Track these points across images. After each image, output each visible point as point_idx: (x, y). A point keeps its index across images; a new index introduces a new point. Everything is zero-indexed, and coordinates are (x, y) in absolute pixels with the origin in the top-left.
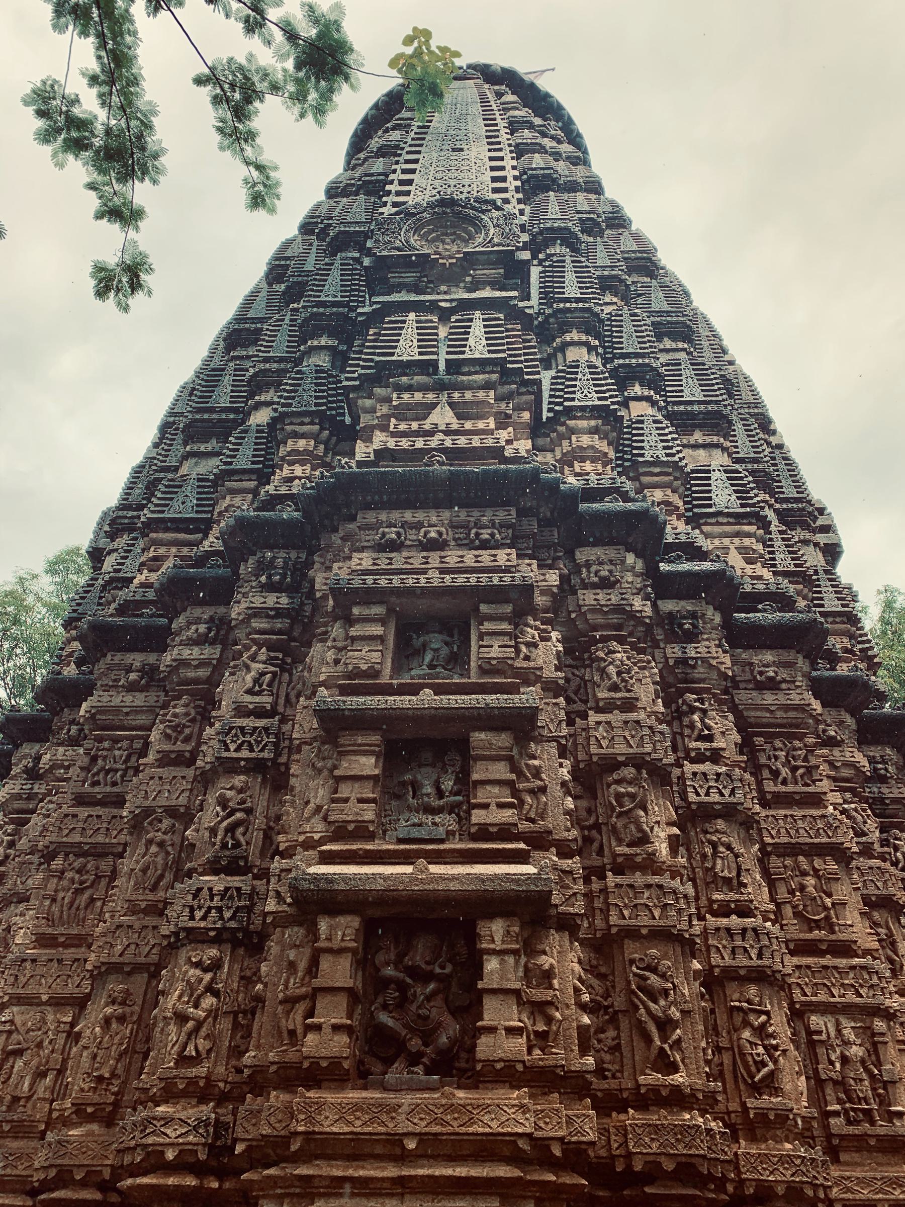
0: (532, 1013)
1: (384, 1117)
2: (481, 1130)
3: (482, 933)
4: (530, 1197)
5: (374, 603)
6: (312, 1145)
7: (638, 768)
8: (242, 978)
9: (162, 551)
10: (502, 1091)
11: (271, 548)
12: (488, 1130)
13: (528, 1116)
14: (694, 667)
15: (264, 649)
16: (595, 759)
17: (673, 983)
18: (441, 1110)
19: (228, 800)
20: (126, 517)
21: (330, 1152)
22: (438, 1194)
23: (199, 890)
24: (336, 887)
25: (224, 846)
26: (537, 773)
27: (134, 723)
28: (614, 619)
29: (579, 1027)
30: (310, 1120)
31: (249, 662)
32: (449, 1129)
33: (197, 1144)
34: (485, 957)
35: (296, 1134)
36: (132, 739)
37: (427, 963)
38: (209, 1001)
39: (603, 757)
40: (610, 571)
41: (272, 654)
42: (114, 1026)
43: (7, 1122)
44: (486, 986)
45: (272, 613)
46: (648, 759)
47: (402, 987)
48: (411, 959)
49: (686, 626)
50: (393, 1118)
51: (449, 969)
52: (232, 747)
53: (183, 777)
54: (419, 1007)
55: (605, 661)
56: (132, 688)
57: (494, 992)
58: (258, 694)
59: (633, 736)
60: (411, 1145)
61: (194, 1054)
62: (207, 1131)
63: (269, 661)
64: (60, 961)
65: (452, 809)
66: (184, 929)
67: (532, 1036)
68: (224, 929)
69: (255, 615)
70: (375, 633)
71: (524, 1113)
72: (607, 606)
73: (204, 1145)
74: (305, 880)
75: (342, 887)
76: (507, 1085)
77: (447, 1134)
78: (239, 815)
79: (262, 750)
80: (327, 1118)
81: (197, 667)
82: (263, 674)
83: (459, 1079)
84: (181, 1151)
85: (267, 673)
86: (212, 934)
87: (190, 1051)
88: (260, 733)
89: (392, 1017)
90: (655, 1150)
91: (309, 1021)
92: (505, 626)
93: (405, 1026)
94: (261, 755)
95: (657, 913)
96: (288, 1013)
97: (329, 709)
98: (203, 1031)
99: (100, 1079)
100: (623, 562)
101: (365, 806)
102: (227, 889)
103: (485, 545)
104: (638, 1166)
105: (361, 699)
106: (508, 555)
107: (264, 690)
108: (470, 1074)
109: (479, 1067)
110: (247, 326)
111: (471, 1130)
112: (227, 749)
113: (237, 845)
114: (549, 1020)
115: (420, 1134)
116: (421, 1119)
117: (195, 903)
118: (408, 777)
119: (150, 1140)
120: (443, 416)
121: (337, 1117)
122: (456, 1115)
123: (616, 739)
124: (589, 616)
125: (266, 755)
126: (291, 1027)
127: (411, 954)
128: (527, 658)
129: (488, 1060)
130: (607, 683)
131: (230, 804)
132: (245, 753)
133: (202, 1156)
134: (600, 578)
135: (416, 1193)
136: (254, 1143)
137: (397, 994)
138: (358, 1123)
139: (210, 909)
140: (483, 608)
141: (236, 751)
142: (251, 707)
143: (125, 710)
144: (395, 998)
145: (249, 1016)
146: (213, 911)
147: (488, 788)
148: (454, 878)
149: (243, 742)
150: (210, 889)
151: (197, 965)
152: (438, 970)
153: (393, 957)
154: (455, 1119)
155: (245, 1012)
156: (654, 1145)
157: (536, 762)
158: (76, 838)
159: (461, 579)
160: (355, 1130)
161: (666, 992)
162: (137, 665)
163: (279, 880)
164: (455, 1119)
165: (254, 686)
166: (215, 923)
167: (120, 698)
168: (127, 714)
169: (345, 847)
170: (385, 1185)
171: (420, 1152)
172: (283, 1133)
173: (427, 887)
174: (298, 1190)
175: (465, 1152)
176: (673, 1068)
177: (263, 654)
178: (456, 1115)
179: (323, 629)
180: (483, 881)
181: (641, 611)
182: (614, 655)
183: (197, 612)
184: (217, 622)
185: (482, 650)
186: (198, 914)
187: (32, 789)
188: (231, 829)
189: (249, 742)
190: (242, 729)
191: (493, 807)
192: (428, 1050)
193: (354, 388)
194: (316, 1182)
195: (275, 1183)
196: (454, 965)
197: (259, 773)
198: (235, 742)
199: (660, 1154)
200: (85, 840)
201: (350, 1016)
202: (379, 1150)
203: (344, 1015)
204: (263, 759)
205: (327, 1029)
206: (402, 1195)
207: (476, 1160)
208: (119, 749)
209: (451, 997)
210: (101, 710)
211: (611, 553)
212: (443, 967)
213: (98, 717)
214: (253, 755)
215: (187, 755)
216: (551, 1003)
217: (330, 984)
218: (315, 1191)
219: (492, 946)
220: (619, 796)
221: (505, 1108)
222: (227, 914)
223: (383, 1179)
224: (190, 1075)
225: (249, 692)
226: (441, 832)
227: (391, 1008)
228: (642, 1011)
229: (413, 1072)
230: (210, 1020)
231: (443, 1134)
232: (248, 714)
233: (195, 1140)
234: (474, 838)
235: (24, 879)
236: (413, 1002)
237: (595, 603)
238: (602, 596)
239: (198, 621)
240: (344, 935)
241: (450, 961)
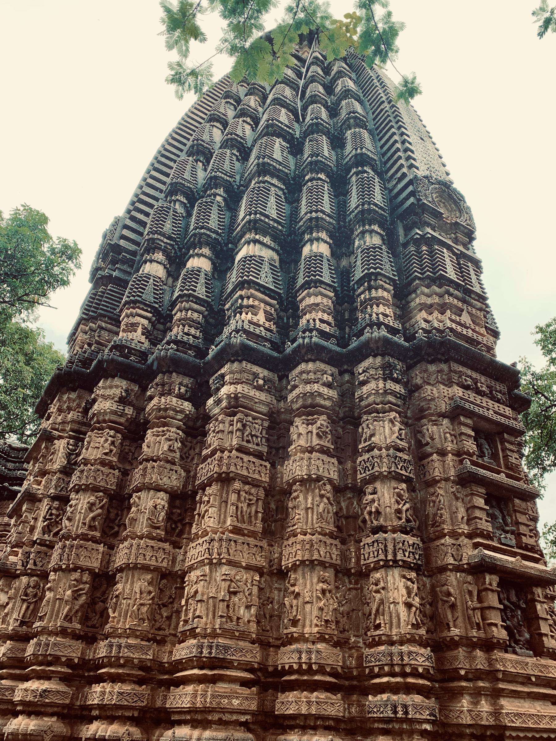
9: (256, 303)
11: (392, 357)
20: (162, 241)
27: (259, 409)
30: (504, 666)
32: (543, 675)
35: (501, 670)
36: (263, 420)
42: (328, 594)
43: (238, 631)
47: (512, 611)
56: (259, 388)
64: (248, 544)
65: (513, 533)
69: (390, 394)
81: (325, 399)
99: (327, 621)
103: (498, 401)
110: (274, 164)
119: (413, 662)
120: (465, 318)
132: (403, 472)
143: (257, 400)
148: (532, 568)
158: (245, 473)
162: (261, 375)
167: (253, 393)
168: (256, 403)
183: (323, 366)
187: (124, 410)
190: (401, 458)
193: (419, 279)
200: (249, 475)
208: (256, 423)
210: (245, 396)
213: (241, 399)
214: (407, 474)
233: (429, 664)
235: (162, 477)
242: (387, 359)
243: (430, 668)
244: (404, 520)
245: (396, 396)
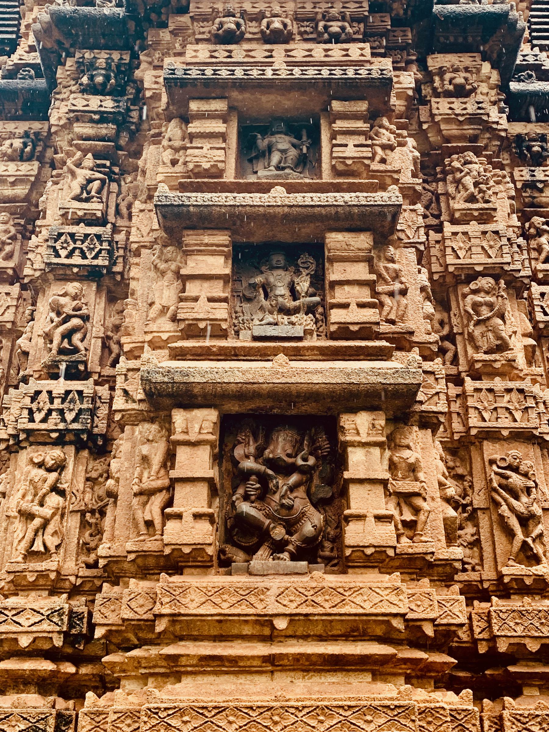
0: (399, 504)
1: (252, 599)
2: (353, 611)
3: (346, 427)
4: (400, 674)
5: (214, 98)
6: (178, 627)
7: (496, 278)
8: (88, 479)
10: (373, 576)
11: (91, 48)
12: (361, 611)
13: (401, 597)
14: (541, 191)
15: (90, 155)
16: (451, 269)
17: (534, 481)
18: (312, 592)
19: (62, 306)
21: (196, 633)
22: (307, 671)
23: (38, 393)
24: (192, 380)
25: (61, 351)
26: (396, 276)
28: (469, 130)
29: (445, 519)
30: (174, 601)
31: (74, 168)
32: (320, 610)
33: (53, 632)
34: (350, 449)
35: (161, 616)
37: (289, 456)
38: (54, 500)
39: (460, 268)
40: (466, 79)
41: (99, 162)
44: (353, 477)
45: (97, 117)
46: (506, 268)
47: (263, 479)
48: (272, 452)
49: (536, 149)
50: (261, 600)
51: (311, 461)
52: (63, 253)
53: (8, 294)
54: (283, 497)
55: (461, 171)
57: (361, 481)
58: (87, 200)
59: (491, 247)
60: (281, 624)
61: (42, 549)
62: (62, 620)
63: (96, 168)
65: (310, 310)
66: (24, 431)
67: (400, 526)
68: (67, 430)
69: (77, 119)
70: (217, 130)
71: (398, 595)
72: (463, 115)
73: (59, 632)
74: (158, 373)
75: (198, 379)
76: (377, 570)
77: (319, 615)
78: (76, 321)
79: (96, 257)
80: (192, 601)
81: (13, 184)
82: (90, 181)
83: (326, 566)
84: (35, 639)
85: (96, 179)
86: (54, 435)
87: (38, 546)
88: (92, 240)
89: (255, 507)
90: (519, 633)
91: (168, 510)
92: (360, 125)
93: (267, 516)
94: (95, 262)
95: (518, 415)
96: (145, 504)
97: (172, 205)
98: (50, 529)
100: (479, 71)
101: (216, 305)
102: (68, 392)
103: (336, 38)
104: (502, 647)
105: (208, 195)
106: (362, 49)
107: (93, 197)
108: (336, 561)
109: (348, 552)
111: (343, 611)
112: (58, 256)
113: (76, 350)
114: (417, 511)
115: (291, 615)
116: (291, 601)
117: (34, 406)
118: (259, 279)
121: (203, 600)
122: (327, 597)
123: (473, 249)
124: (443, 127)
125: (99, 262)
126: (148, 517)
127: (272, 447)
128: (383, 161)
129: (358, 546)
130: (464, 194)
131: (65, 310)
132: (77, 260)
133: (58, 642)
134: (456, 86)
135: (286, 670)
136: (114, 628)
137: (258, 485)
138: (225, 605)
139: (50, 411)
140: (336, 105)
141: (67, 257)
142: (80, 213)
144: (257, 489)
145: (97, 515)
146: (54, 413)
147: (346, 288)
149: (74, 249)
150: (50, 393)
151: (40, 465)
152: (300, 462)
153: (252, 449)
154: (327, 601)
155: (93, 512)
156: (519, 629)
157: (396, 266)
159: (311, 72)
160: (223, 612)
161: (528, 491)
163: (126, 380)
164: (327, 601)
165: (82, 193)
166: (56, 424)
169: (197, 345)
170: (255, 663)
171: (290, 633)
172: (145, 617)
173: (289, 380)
174: (162, 670)
175: (335, 632)
176: (536, 560)
177: (89, 160)
178: (327, 597)
179: (157, 131)
180: (348, 375)
181: (497, 123)
182: (470, 166)
184: (32, 136)
185: (335, 149)
186: (38, 417)
188: (68, 335)
189: (81, 249)
190: (72, 235)
191: (353, 306)
192: (294, 538)
194: (183, 661)
195: (139, 662)
196: (317, 458)
197: (93, 281)
198: (66, 248)
199: (524, 637)
201: (210, 506)
202: (247, 630)
203: (206, 506)
204: (97, 266)
205: (188, 517)
206: (272, 672)
207: (346, 640)
209: (313, 489)
211: (466, 60)
212: (305, 459)
214: (86, 262)
215: (10, 272)
216: (418, 495)
217: (190, 475)
218: (183, 669)
219: (357, 439)
220: (476, 306)
221: (378, 590)
222: (69, 416)
223: (253, 657)
224: (39, 569)
225: (77, 198)
226: (298, 331)
227: (253, 498)
228: (504, 507)
229: (279, 558)
230: (57, 517)
231: (315, 615)
232: (78, 221)
234: (333, 336)
236: (275, 493)
237: (450, 112)
238: (457, 105)
239: (12, 135)
240: (201, 428)
241: (311, 454)
242: (78, 55)
243: (55, 636)
244: (54, 352)
245: (92, 121)
